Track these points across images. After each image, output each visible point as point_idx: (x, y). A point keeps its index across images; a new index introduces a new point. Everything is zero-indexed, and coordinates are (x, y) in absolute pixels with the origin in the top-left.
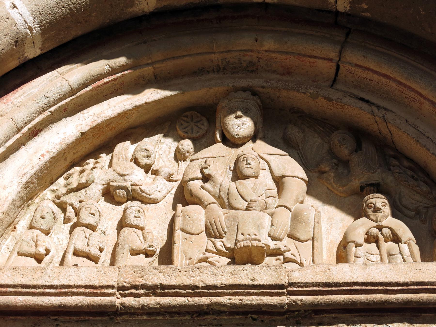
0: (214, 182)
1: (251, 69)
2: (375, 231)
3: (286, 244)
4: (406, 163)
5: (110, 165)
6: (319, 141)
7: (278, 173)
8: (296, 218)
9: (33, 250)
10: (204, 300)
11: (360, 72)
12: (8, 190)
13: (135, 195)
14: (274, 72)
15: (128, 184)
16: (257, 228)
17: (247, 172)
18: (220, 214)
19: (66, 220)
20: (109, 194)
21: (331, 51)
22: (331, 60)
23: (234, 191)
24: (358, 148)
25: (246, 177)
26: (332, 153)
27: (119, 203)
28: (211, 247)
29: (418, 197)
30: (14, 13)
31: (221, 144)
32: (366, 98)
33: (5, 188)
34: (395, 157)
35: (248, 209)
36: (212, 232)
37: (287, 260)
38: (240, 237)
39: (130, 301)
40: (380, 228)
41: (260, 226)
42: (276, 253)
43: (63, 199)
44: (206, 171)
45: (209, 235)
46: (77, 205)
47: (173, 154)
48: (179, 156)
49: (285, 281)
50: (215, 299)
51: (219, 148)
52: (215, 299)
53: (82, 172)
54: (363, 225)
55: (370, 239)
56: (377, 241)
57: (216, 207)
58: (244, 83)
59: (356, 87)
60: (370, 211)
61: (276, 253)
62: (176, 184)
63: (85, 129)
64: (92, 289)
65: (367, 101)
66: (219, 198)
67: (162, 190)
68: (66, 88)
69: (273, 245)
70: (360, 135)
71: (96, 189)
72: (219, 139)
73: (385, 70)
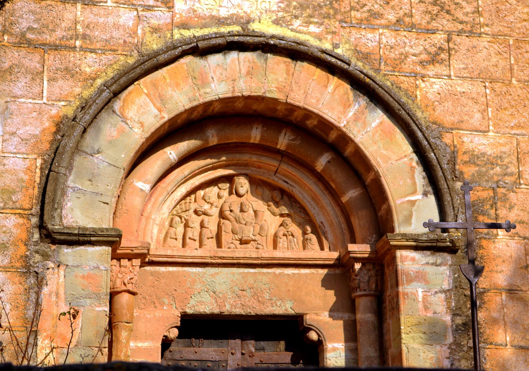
0: (234, 213)
1: (246, 165)
2: (286, 233)
3: (258, 237)
4: (298, 205)
5: (195, 201)
6: (268, 192)
7: (255, 209)
8: (261, 228)
9: (175, 237)
10: (235, 261)
11: (285, 172)
12: (165, 215)
13: (205, 214)
14: (255, 167)
15: (203, 210)
16: (249, 233)
17: (245, 210)
18: (237, 225)
19: (182, 222)
20: (196, 212)
21: (276, 163)
22: (275, 167)
23: (241, 217)
24: (282, 198)
25: (244, 212)
26: (272, 197)
27: (199, 216)
28: (234, 238)
29: (301, 219)
30: (171, 156)
31: (235, 195)
32: (287, 181)
33: (164, 214)
34: (294, 202)
35: (245, 225)
36: (234, 232)
37: (258, 244)
38: (244, 235)
39: (214, 261)
40: (288, 232)
41: (249, 232)
42: (255, 241)
43: (180, 214)
44: (231, 208)
45: (233, 233)
46: (185, 217)
47: (217, 196)
48: (219, 197)
49: (260, 256)
50: (239, 261)
51: (234, 196)
52: (239, 261)
53: (186, 203)
54: (282, 231)
55: (284, 235)
56: (286, 236)
57: (235, 222)
58: (244, 172)
59: (283, 176)
60: (285, 225)
61: (255, 241)
62: (219, 209)
63: (189, 190)
64: (202, 257)
65: (287, 182)
66: (236, 219)
67: (215, 212)
68: (184, 176)
69: (254, 238)
70: (283, 192)
71: (192, 211)
72: (234, 193)
73: (294, 174)
